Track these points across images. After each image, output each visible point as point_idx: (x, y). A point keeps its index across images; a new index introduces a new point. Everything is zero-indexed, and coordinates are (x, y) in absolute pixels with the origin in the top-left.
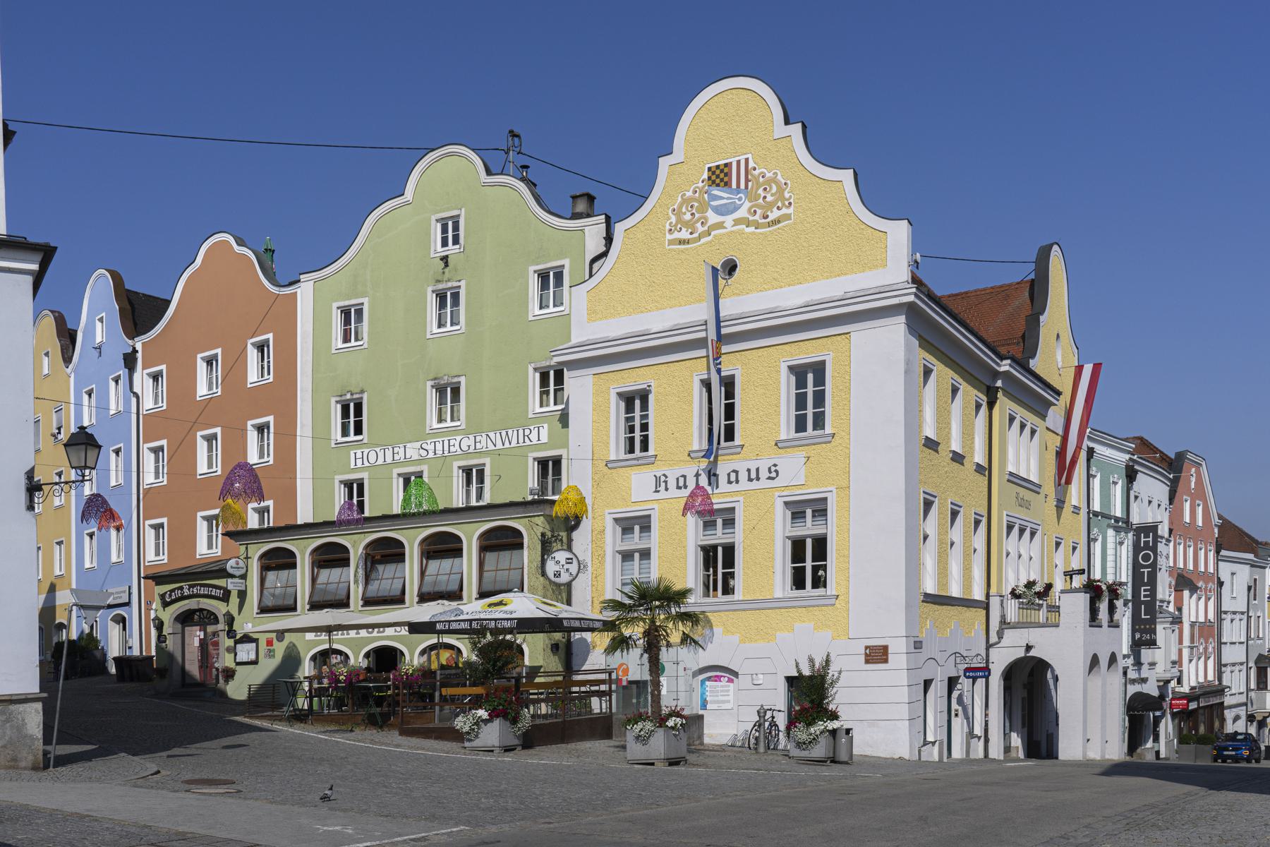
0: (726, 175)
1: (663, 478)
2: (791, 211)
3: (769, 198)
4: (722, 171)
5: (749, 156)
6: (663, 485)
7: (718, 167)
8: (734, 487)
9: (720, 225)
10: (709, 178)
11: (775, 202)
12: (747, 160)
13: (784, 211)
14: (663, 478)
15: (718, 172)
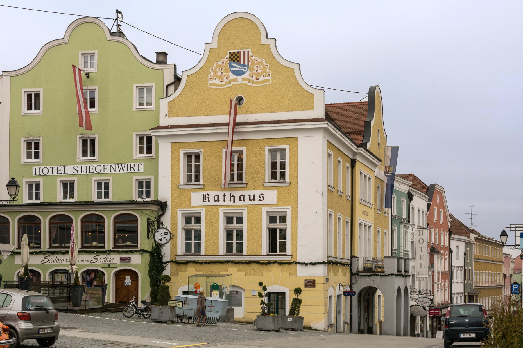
0: (238, 57)
1: (207, 196)
2: (269, 78)
3: (259, 71)
4: (236, 55)
5: (250, 50)
6: (207, 199)
7: (234, 53)
8: (242, 203)
9: (235, 80)
10: (230, 57)
11: (262, 73)
12: (248, 52)
13: (266, 78)
14: (207, 196)
15: (234, 55)
